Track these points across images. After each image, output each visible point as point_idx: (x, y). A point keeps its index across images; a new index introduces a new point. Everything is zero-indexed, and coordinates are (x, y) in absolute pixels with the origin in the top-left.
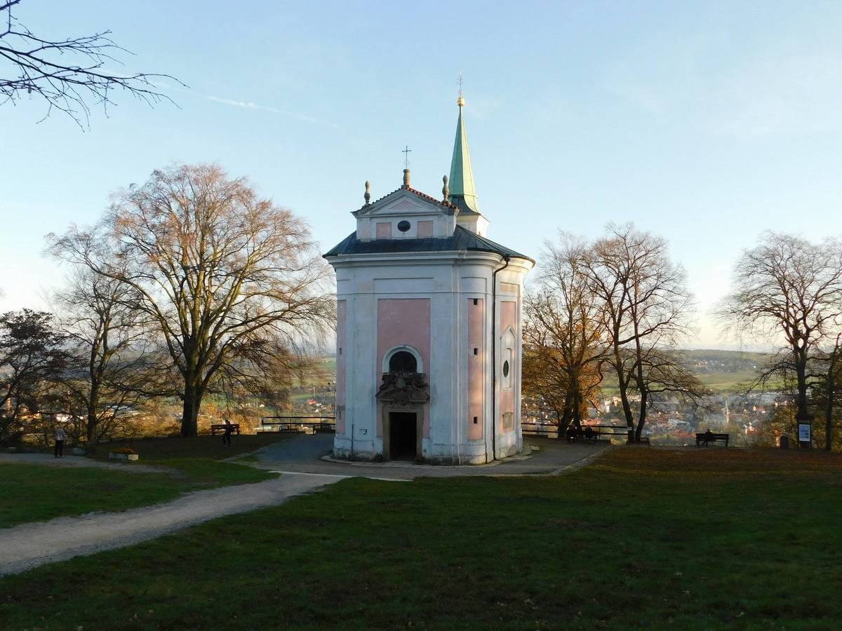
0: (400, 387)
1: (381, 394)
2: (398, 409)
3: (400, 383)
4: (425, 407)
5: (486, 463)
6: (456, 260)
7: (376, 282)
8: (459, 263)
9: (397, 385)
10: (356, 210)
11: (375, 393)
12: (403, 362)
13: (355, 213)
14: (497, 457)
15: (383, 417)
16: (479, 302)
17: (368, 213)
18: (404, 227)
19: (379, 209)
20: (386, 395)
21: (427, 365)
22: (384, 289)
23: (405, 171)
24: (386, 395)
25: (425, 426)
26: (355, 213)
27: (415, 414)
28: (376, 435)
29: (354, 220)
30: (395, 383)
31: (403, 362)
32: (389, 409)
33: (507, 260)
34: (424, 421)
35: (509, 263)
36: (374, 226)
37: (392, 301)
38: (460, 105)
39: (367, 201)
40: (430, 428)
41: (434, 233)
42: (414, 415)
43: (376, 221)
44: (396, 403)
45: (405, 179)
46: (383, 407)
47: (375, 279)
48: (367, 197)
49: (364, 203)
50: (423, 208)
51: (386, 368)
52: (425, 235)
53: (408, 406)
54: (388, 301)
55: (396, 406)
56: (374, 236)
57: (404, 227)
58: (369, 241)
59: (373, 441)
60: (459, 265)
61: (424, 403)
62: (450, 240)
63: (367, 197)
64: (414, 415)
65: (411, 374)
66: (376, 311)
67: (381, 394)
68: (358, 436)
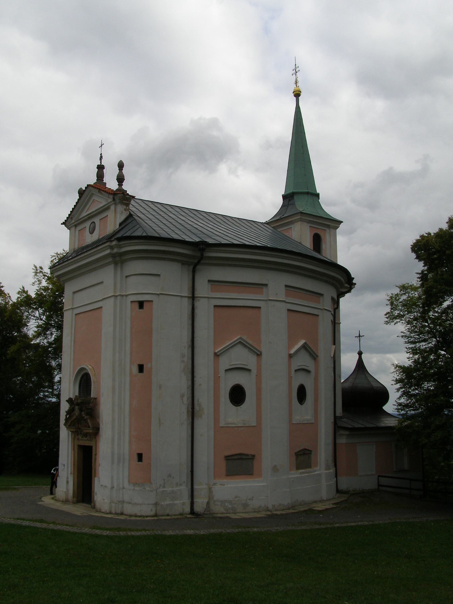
1: (69, 424)
6: (113, 256)
7: (76, 295)
16: (145, 304)
28: (70, 472)
29: (65, 233)
33: (202, 250)
34: (97, 456)
36: (77, 232)
38: (297, 95)
42: (91, 447)
54: (81, 315)
60: (123, 262)
64: (91, 447)
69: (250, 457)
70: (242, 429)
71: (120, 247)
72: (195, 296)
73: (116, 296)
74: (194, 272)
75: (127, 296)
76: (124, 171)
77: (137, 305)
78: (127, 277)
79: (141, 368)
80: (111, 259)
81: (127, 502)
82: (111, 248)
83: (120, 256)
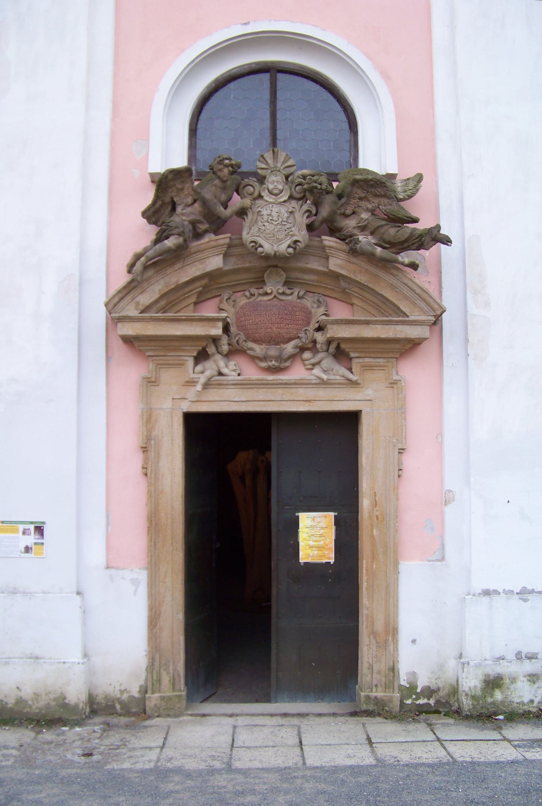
0: (268, 247)
1: (146, 298)
4: (411, 371)
21: (418, 127)
24: (170, 301)
27: (351, 420)
34: (410, 462)
40: (447, 499)
44: (234, 352)
46: (150, 383)
53: (298, 372)
55: (230, 368)
61: (409, 347)
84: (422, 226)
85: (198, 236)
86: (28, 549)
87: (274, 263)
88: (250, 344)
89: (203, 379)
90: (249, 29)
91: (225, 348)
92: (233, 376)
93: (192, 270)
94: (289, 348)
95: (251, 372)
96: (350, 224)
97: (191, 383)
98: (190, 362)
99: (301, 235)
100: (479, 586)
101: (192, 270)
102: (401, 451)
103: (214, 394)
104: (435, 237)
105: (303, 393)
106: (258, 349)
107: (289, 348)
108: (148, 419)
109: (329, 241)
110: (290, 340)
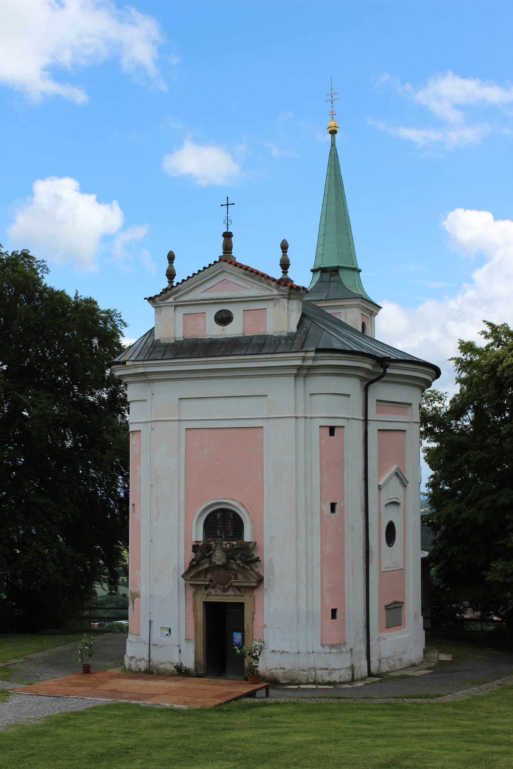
0: (217, 563)
1: (191, 575)
2: (217, 597)
3: (219, 557)
4: (257, 593)
5: (353, 680)
6: (300, 368)
7: (183, 403)
8: (305, 372)
9: (213, 560)
10: (153, 295)
11: (183, 571)
12: (223, 524)
13: (151, 300)
14: (373, 669)
15: (195, 609)
16: (336, 431)
17: (171, 300)
18: (224, 318)
19: (186, 293)
20: (197, 576)
22: (197, 412)
23: (228, 235)
25: (257, 623)
26: (151, 300)
27: (242, 604)
28: (183, 636)
30: (210, 557)
31: (223, 524)
32: (201, 598)
33: (385, 367)
34: (256, 616)
35: (389, 371)
37: (206, 432)
38: (333, 132)
39: (171, 281)
40: (265, 626)
41: (268, 328)
42: (241, 605)
43: (181, 312)
44: (214, 587)
45: (228, 248)
46: (195, 594)
47: (180, 399)
48: (171, 275)
49: (165, 284)
50: (253, 290)
51: (198, 535)
52: (253, 331)
53: (230, 592)
54: (202, 431)
55: (213, 591)
56: (180, 335)
57: (224, 318)
58: (173, 341)
59: (179, 646)
60: (306, 376)
62: (291, 337)
63: (171, 275)
64: (241, 605)
65: (235, 543)
66: (183, 450)
67: (191, 575)
68: (157, 636)
69: (400, 605)
70: (396, 572)
71: (314, 359)
72: (368, 419)
73: (297, 418)
74: (366, 390)
75: (311, 418)
76: (290, 253)
77: (328, 430)
78: (311, 394)
79: (333, 506)
80: (295, 371)
81: (321, 669)
82: (304, 359)
83: (308, 369)
84: (255, 557)
85: (202, 559)
86: (167, 635)
87: (219, 567)
88: (217, 585)
89: (206, 593)
90: (215, 501)
91: (212, 586)
92: (214, 593)
93: (201, 568)
94: (226, 586)
95: (219, 592)
96: (236, 557)
97: (204, 594)
98: (204, 589)
99: (224, 560)
100: (272, 649)
101: (201, 568)
102: (254, 613)
103: (209, 597)
104: (258, 560)
105: (230, 597)
106: (219, 586)
107: (226, 586)
108: (195, 603)
109: (232, 561)
110: (226, 584)
